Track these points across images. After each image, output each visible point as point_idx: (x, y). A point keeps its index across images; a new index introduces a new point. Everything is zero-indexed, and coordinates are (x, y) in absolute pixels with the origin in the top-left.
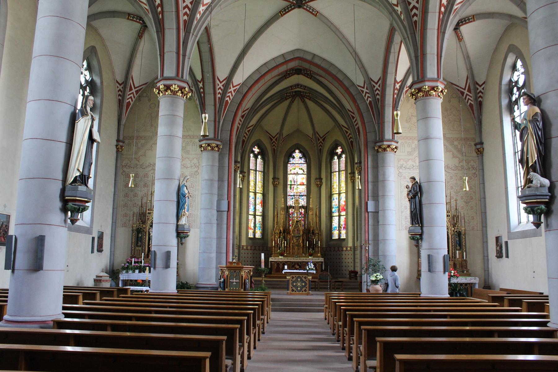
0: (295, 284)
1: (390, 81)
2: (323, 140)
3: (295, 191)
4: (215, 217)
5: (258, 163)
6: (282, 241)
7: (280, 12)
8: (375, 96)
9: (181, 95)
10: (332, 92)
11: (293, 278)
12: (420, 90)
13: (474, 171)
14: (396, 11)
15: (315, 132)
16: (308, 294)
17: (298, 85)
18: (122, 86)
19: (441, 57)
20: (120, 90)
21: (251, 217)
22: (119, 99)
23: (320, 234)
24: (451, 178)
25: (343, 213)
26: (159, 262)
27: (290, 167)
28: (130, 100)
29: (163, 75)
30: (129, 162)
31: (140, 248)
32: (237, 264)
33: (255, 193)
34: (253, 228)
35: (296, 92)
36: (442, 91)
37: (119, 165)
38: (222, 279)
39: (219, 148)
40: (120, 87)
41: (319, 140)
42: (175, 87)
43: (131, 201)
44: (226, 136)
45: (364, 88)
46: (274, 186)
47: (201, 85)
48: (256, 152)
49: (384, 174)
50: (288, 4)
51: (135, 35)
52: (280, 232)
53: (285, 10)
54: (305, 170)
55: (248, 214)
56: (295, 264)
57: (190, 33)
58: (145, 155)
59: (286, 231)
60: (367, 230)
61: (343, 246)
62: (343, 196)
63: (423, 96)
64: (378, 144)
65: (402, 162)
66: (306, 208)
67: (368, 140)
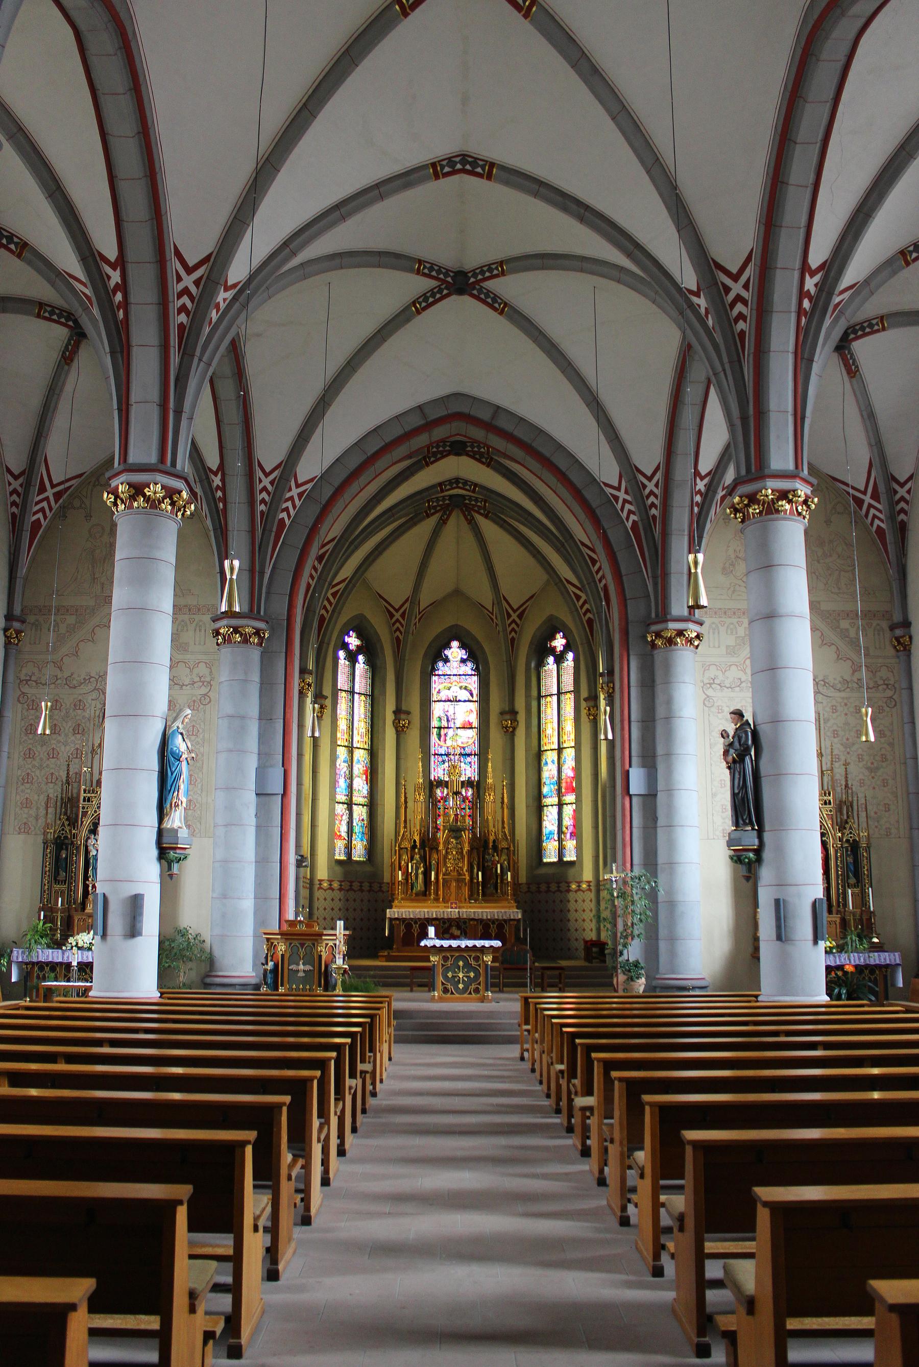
0: (450, 975)
1: (682, 471)
3: (449, 743)
4: (252, 810)
5: (357, 673)
6: (417, 869)
7: (414, 303)
8: (644, 509)
9: (169, 508)
10: (541, 498)
11: (445, 959)
12: (752, 499)
13: (889, 693)
14: (694, 308)
16: (483, 1000)
17: (456, 482)
18: (21, 480)
19: (803, 418)
20: (14, 491)
21: (341, 809)
22: (13, 515)
23: (510, 852)
24: (834, 709)
25: (570, 798)
26: (116, 922)
27: (437, 685)
28: (40, 515)
29: (125, 460)
30: (36, 670)
31: (64, 887)
32: (307, 926)
33: (351, 749)
34: (344, 835)
35: (451, 497)
36: (805, 502)
37: (11, 678)
38: (271, 964)
39: (261, 639)
40: (16, 484)
41: (509, 616)
42: (155, 490)
43: (41, 768)
44: (280, 607)
45: (618, 489)
46: (397, 731)
47: (217, 481)
48: (352, 648)
49: (669, 702)
50: (434, 283)
51: (54, 356)
52: (414, 847)
53: (426, 300)
54: (475, 692)
55: (333, 801)
56: (451, 926)
57: (193, 356)
58: (76, 654)
59: (428, 844)
60: (628, 839)
61: (570, 879)
62: (569, 755)
63: (761, 513)
64: (654, 628)
65: (713, 672)
66: (478, 786)
67: (630, 618)
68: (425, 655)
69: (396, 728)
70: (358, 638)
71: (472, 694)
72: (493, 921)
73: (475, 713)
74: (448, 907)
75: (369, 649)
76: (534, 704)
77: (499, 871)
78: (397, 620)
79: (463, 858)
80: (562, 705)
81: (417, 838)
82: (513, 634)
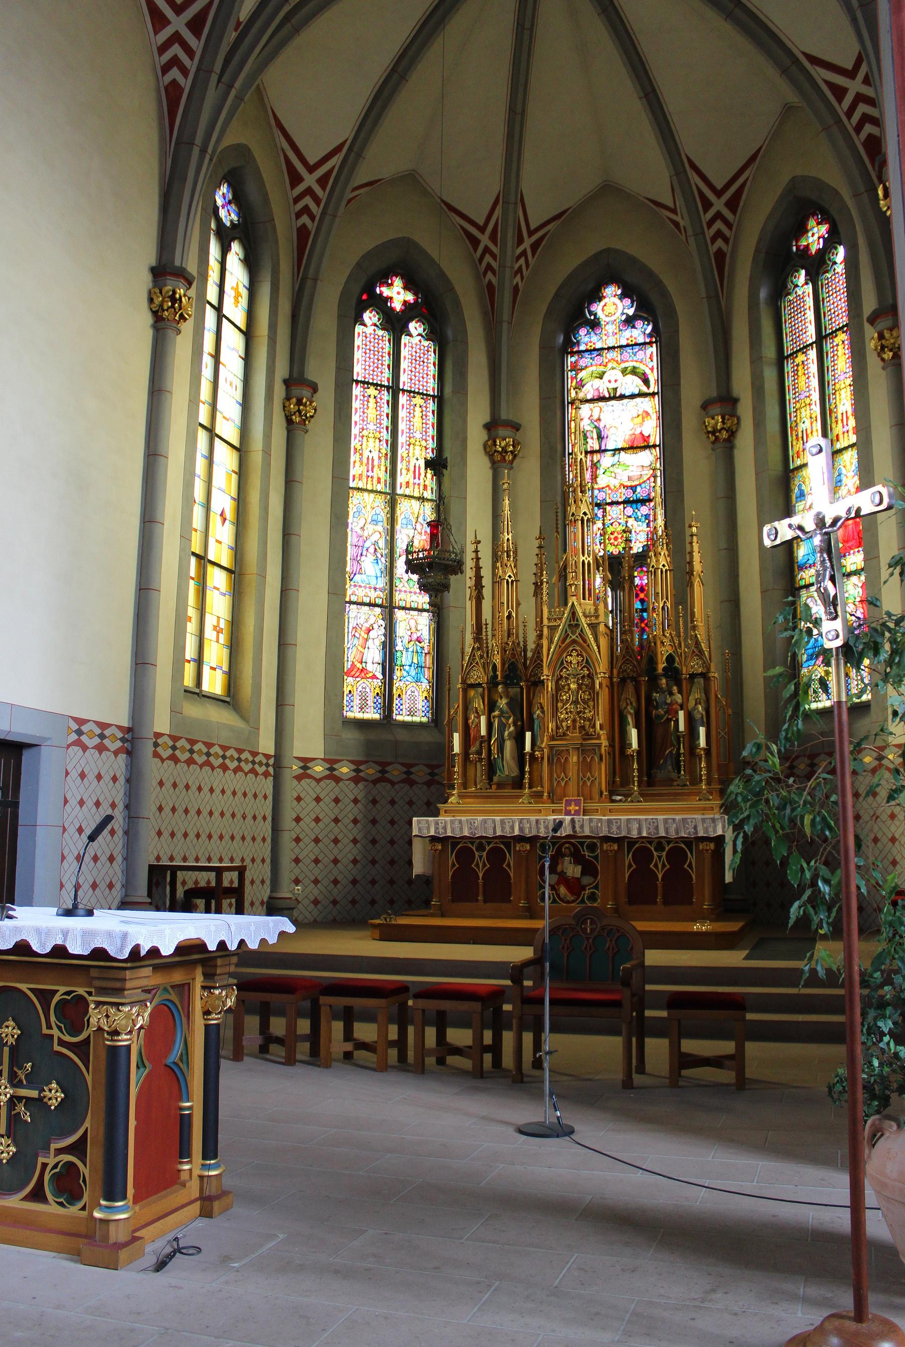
2: (732, 204)
5: (404, 352)
15: (681, 165)
41: (707, 205)
46: (493, 463)
52: (493, 683)
54: (653, 377)
70: (406, 288)
71: (646, 381)
72: (660, 843)
73: (654, 416)
75: (433, 310)
76: (770, 374)
77: (682, 727)
78: (487, 250)
79: (594, 696)
80: (828, 363)
81: (497, 660)
82: (719, 243)
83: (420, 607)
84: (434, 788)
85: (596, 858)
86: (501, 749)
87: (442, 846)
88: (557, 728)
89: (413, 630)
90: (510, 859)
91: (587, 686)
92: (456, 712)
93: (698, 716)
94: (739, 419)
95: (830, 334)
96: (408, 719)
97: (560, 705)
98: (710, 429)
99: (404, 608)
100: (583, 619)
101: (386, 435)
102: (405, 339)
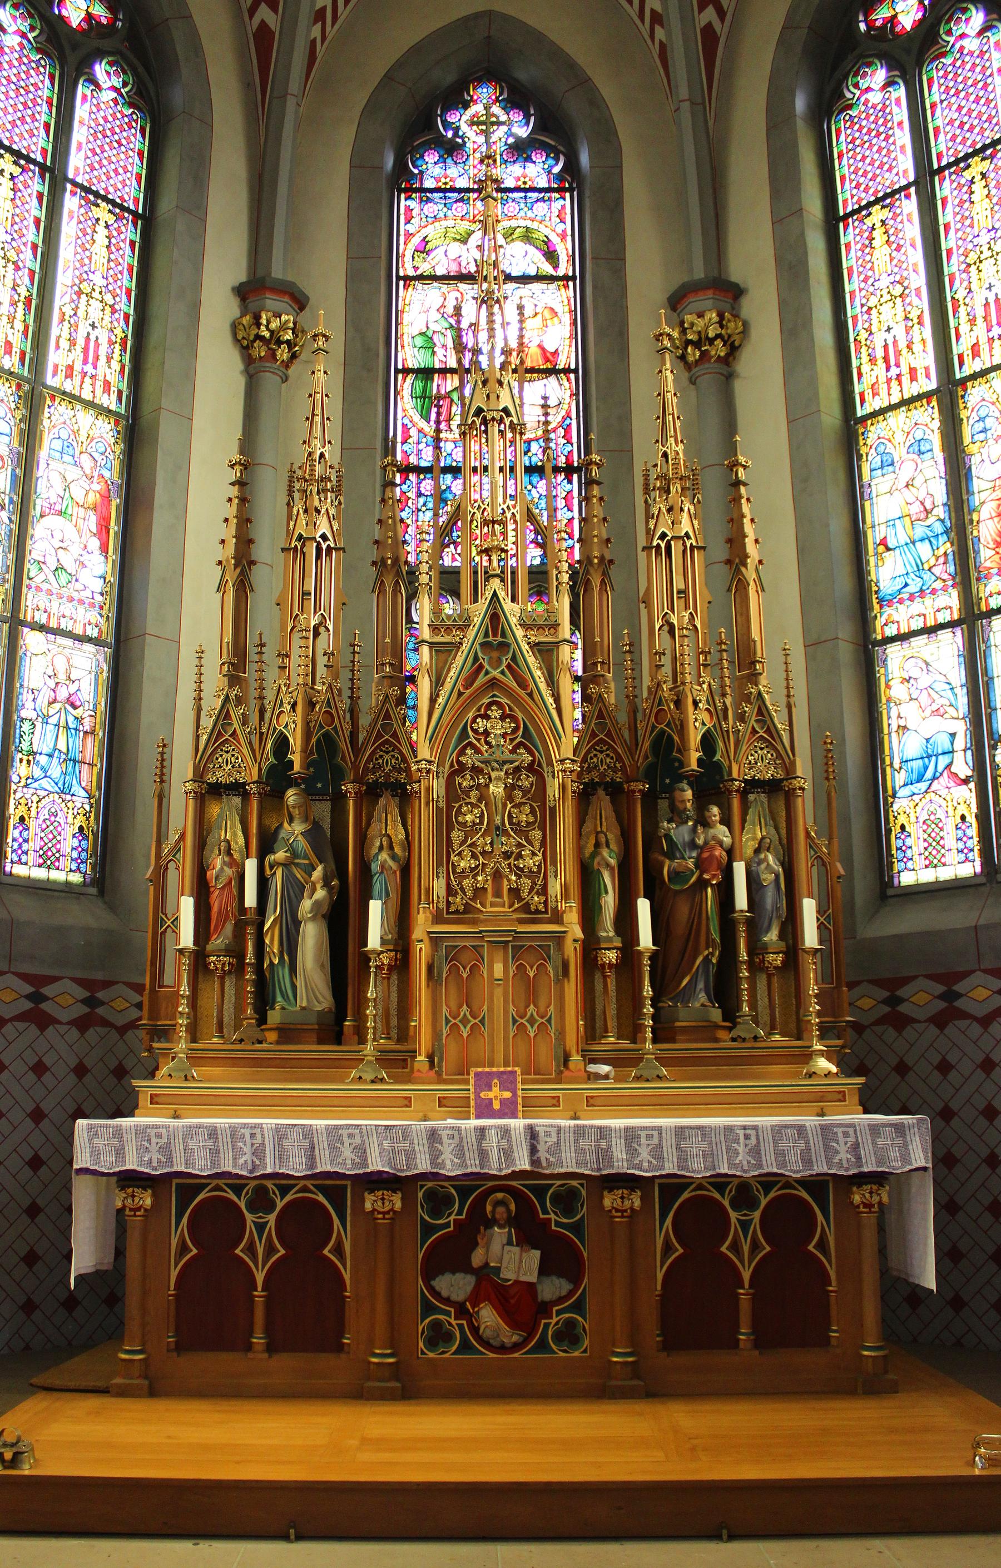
5: (81, 111)
6: (295, 891)
46: (249, 361)
52: (278, 778)
54: (563, 249)
56: (477, 1222)
68: (370, 109)
69: (245, 349)
71: (551, 255)
73: (567, 319)
74: (460, 1107)
77: (741, 901)
81: (292, 726)
83: (79, 631)
84: (92, 1034)
85: (577, 1228)
86: (290, 944)
87: (154, 1195)
88: (450, 891)
89: (62, 677)
90: (343, 1232)
91: (525, 792)
92: (176, 849)
93: (767, 878)
94: (746, 324)
95: (949, 165)
96: (40, 874)
97: (457, 835)
98: (690, 337)
99: (43, 628)
100: (519, 633)
101: (29, 260)
102: (82, 89)
